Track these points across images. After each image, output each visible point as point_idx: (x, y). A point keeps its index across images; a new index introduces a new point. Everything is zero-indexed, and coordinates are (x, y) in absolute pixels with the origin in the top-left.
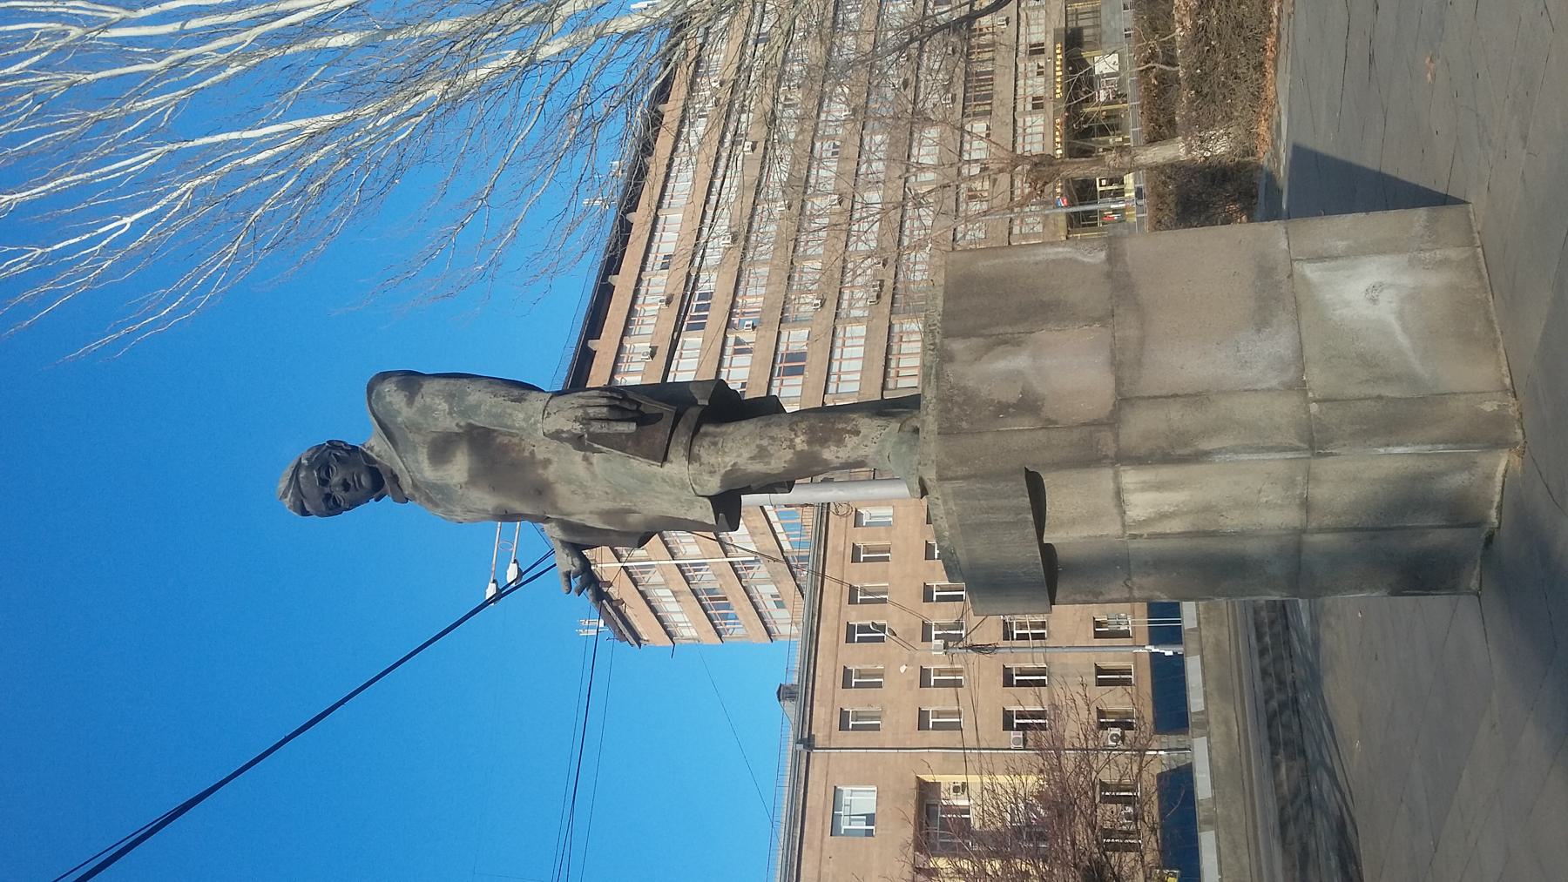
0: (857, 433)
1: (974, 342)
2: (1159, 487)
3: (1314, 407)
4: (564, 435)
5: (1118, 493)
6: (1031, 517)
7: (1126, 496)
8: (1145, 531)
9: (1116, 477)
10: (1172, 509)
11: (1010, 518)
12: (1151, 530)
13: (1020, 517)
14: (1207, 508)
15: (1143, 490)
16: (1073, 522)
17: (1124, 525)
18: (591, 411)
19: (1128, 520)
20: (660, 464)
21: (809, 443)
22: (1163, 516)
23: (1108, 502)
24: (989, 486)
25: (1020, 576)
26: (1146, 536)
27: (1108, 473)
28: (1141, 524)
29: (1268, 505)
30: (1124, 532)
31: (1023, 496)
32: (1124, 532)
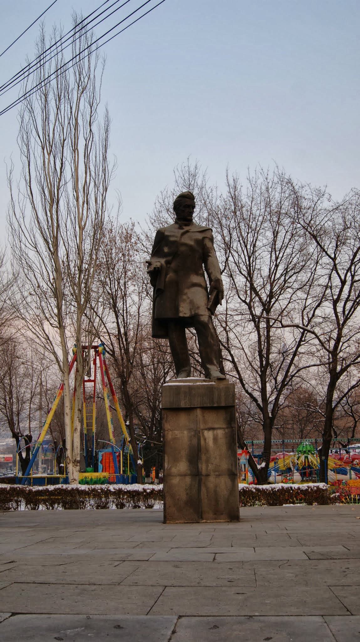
2: (215, 439)
5: (213, 429)
6: (215, 405)
8: (201, 435)
9: (220, 428)
13: (216, 403)
14: (207, 451)
15: (214, 435)
16: (204, 417)
17: (202, 430)
20: (209, 307)
22: (205, 439)
23: (210, 425)
27: (224, 426)
28: (203, 433)
29: (207, 466)
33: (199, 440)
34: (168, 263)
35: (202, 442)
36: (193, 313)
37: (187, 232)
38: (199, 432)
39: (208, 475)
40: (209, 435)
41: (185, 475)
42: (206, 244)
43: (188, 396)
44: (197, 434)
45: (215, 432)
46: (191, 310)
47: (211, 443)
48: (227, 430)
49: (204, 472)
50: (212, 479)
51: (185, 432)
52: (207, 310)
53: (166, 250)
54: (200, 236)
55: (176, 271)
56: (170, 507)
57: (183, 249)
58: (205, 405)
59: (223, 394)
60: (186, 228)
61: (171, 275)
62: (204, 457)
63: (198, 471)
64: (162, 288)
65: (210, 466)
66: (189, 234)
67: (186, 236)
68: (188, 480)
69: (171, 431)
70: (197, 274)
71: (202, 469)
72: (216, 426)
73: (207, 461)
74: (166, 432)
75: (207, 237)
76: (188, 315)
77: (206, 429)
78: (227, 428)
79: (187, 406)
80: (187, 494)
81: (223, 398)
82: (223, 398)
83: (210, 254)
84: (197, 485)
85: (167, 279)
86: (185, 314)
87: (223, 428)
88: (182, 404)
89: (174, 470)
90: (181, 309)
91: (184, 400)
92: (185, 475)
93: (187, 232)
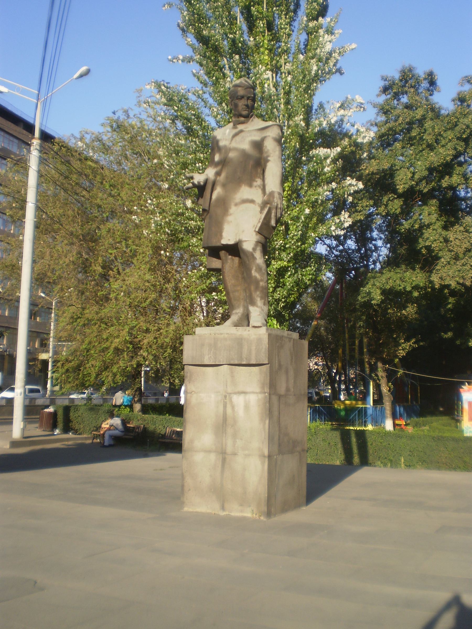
0: (264, 304)
1: (292, 349)
2: (247, 407)
3: (275, 457)
4: (271, 199)
6: (244, 363)
7: (243, 395)
8: (227, 400)
9: (253, 393)
10: (236, 410)
11: (244, 356)
12: (228, 403)
13: (245, 359)
14: (235, 421)
17: (230, 393)
18: (279, 211)
19: (232, 395)
20: (257, 230)
21: (262, 287)
22: (233, 407)
23: (240, 388)
24: (263, 350)
25: (208, 355)
26: (225, 400)
27: (258, 390)
29: (234, 442)
30: (228, 393)
31: (257, 362)
32: (228, 393)
33: (225, 407)
34: (218, 174)
35: (229, 411)
36: (237, 240)
37: (241, 131)
38: (225, 397)
39: (235, 454)
40: (239, 400)
41: (209, 451)
42: (266, 147)
43: (213, 349)
45: (248, 396)
47: (241, 412)
48: (261, 396)
49: (229, 449)
50: (240, 459)
51: (213, 396)
52: (254, 233)
54: (257, 137)
56: (190, 490)
57: (232, 155)
58: (232, 362)
59: (253, 348)
60: (240, 127)
61: (218, 191)
62: (230, 431)
64: (207, 208)
65: (239, 443)
66: (242, 134)
67: (238, 138)
68: (213, 457)
69: (195, 393)
70: (251, 186)
71: (226, 445)
72: (248, 390)
73: (235, 436)
74: (189, 395)
75: (269, 136)
76: (231, 242)
77: (235, 393)
78: (261, 393)
79: (211, 363)
80: (211, 476)
81: (254, 352)
82: (254, 352)
83: (269, 158)
84: (220, 466)
85: (214, 197)
86: (229, 240)
87: (257, 393)
88: (205, 360)
89: (197, 444)
90: (224, 234)
91: (208, 355)
92: (209, 451)
93: (241, 131)
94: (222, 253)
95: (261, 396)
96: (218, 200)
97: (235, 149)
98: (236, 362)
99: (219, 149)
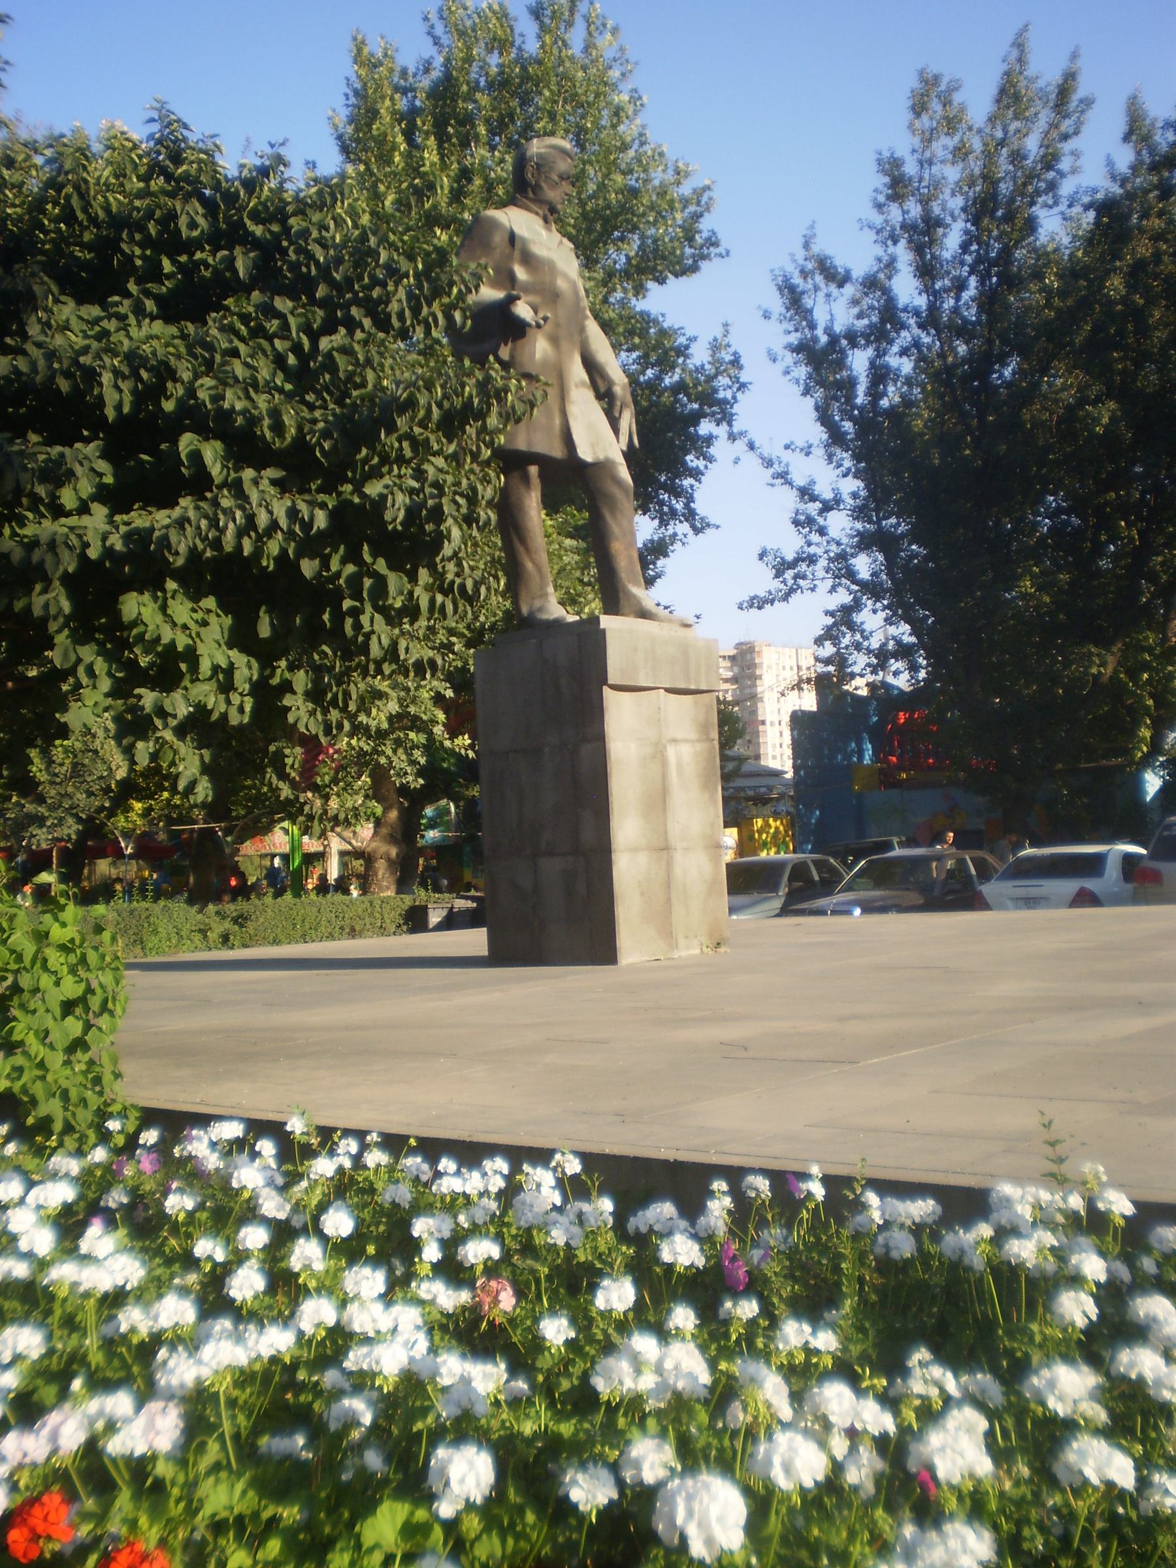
2: (679, 766)
6: (693, 687)
9: (686, 741)
27: (693, 736)
36: (601, 457)
40: (671, 752)
41: (635, 850)
44: (658, 755)
46: (593, 445)
48: (699, 747)
51: (633, 746)
53: (521, 273)
55: (554, 340)
57: (561, 284)
63: (666, 839)
68: (643, 859)
72: (679, 736)
78: (699, 741)
80: (642, 894)
92: (635, 850)
94: (533, 470)
95: (699, 747)
96: (545, 363)
97: (566, 277)
98: (682, 685)
99: (528, 259)
